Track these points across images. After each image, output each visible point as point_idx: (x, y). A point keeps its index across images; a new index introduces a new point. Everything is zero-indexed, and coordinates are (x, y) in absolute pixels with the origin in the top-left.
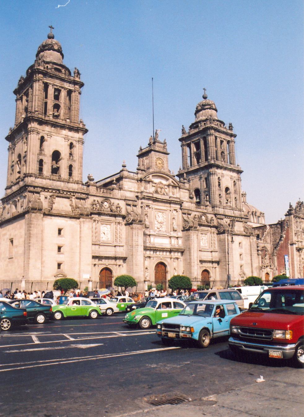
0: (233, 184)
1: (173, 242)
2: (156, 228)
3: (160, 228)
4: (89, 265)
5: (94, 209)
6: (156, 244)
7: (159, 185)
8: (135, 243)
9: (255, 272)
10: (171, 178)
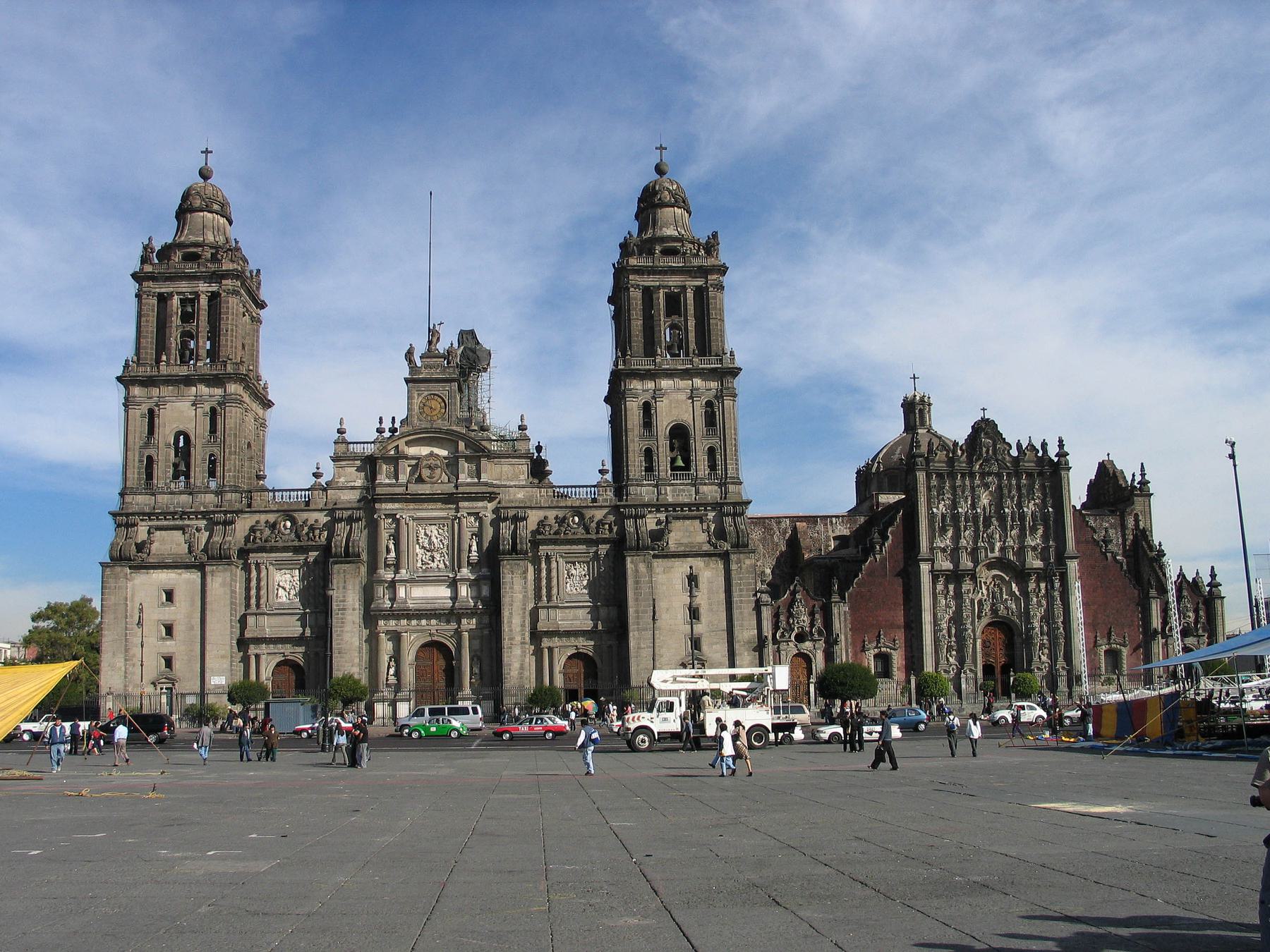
0: (700, 411)
1: (464, 591)
2: (419, 564)
3: (430, 562)
4: (223, 657)
5: (258, 541)
6: (409, 601)
7: (425, 463)
8: (337, 605)
9: (746, 654)
10: (463, 439)
